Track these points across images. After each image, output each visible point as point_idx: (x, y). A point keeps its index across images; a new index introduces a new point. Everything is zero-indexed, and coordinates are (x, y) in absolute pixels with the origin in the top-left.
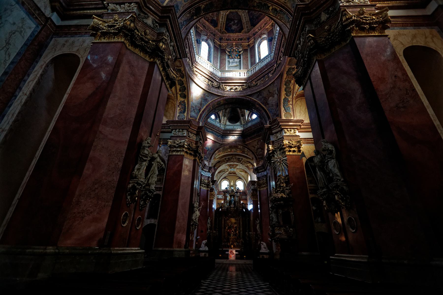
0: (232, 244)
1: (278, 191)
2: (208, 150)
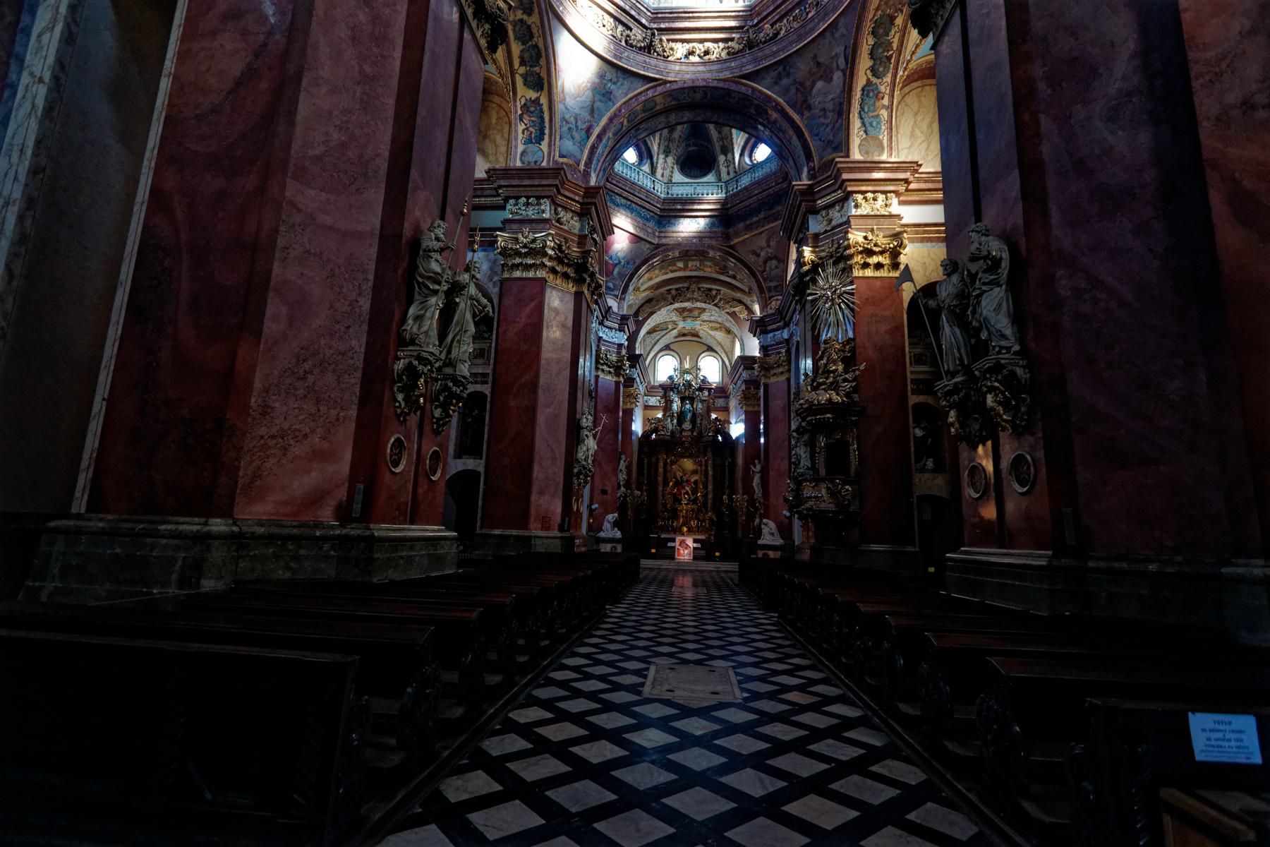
0: (684, 524)
1: (820, 384)
2: (616, 265)
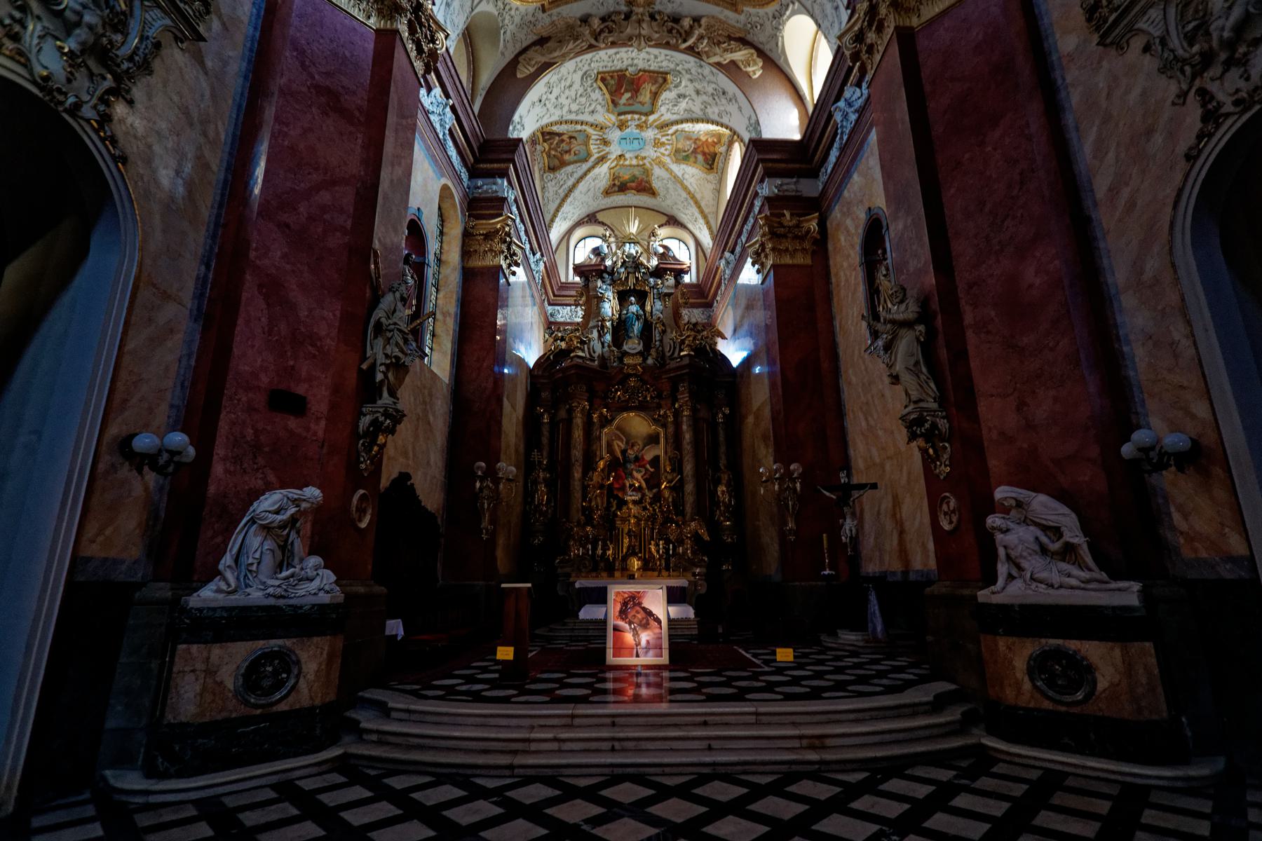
0: (632, 552)
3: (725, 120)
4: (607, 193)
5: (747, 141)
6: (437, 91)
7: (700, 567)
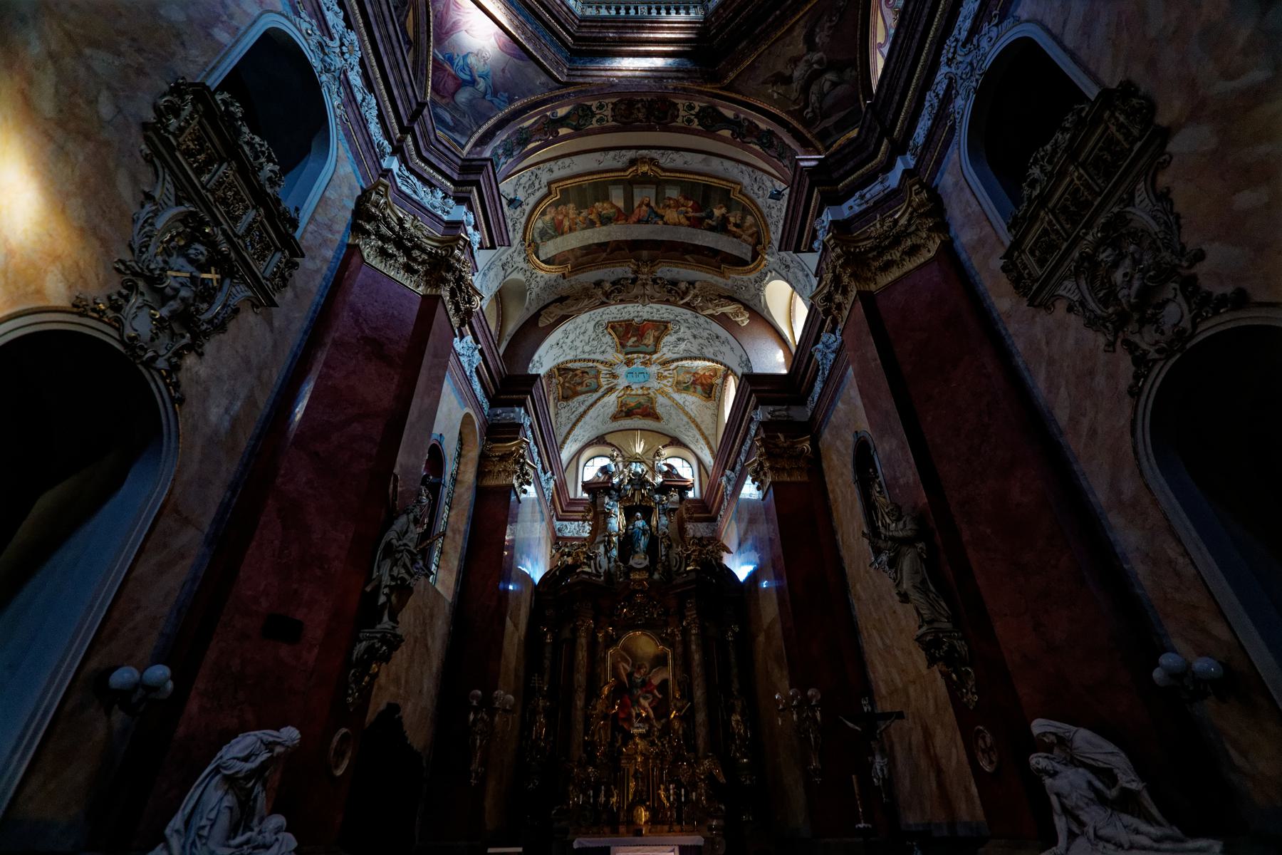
0: (639, 800)
3: (720, 358)
4: (615, 418)
5: (740, 375)
6: (469, 338)
7: (717, 818)
